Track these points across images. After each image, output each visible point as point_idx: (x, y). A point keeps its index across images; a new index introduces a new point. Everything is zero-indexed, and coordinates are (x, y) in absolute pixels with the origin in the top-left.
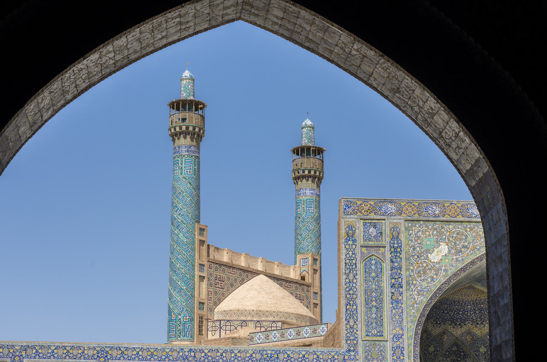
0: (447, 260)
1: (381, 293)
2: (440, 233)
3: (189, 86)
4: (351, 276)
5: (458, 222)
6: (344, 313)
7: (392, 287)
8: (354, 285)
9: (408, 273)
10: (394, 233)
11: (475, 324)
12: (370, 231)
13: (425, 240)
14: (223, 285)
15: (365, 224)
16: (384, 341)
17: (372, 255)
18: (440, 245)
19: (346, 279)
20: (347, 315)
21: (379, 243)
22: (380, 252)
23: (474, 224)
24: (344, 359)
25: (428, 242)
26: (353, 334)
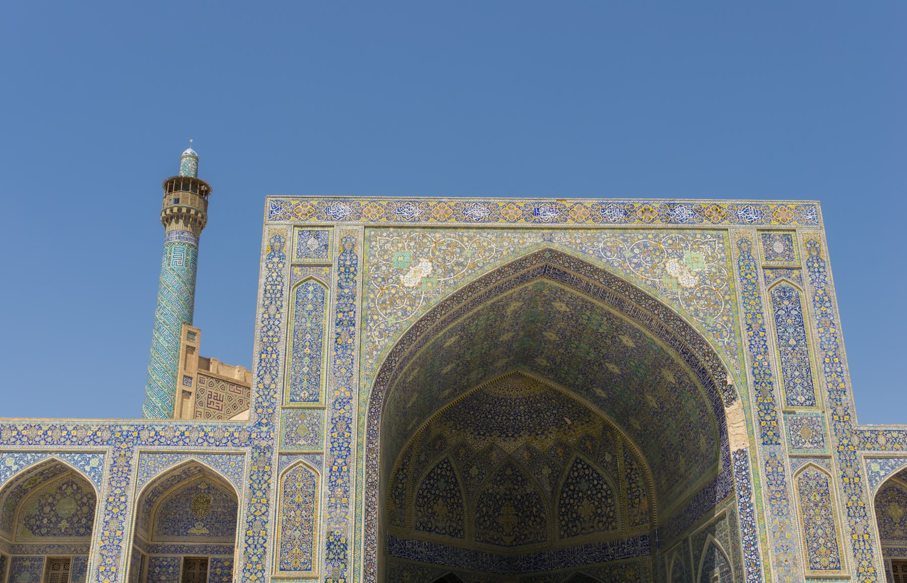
0: (429, 285)
1: (321, 335)
2: (420, 245)
6: (256, 366)
7: (337, 325)
8: (277, 323)
9: (365, 304)
10: (346, 246)
11: (534, 434)
13: (396, 254)
15: (301, 234)
16: (320, 408)
17: (309, 279)
19: (265, 313)
21: (322, 261)
24: (250, 438)
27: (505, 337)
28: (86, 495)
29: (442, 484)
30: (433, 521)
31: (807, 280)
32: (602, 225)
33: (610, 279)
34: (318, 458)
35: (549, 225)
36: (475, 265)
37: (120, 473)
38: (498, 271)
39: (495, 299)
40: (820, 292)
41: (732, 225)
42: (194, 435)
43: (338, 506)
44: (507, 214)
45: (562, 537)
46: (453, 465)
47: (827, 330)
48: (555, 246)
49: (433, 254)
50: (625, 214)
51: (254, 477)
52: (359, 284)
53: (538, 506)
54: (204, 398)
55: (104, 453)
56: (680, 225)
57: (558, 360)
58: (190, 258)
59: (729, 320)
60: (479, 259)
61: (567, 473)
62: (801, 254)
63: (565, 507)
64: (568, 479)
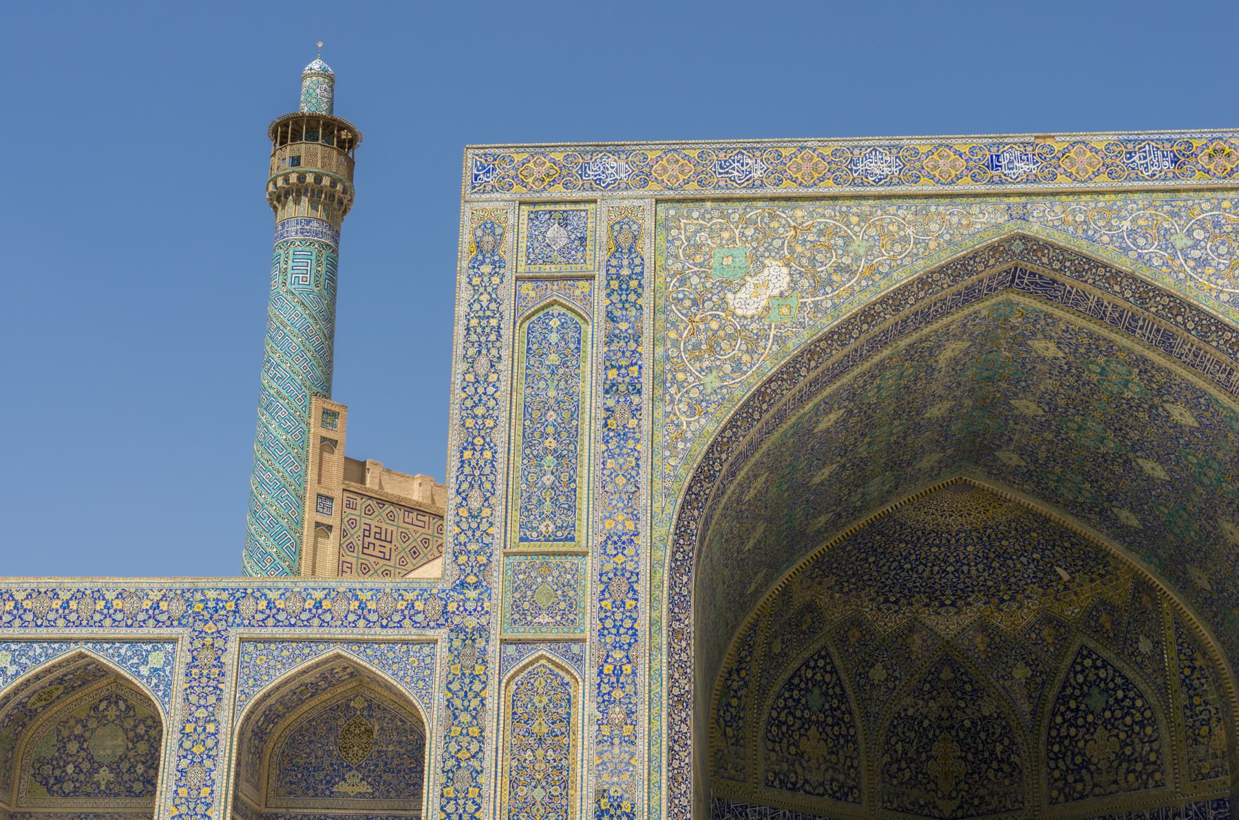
0: (785, 310)
1: (576, 412)
2: (765, 233)
3: (318, 91)
4: (482, 364)
5: (822, 198)
6: (454, 474)
7: (607, 392)
8: (491, 390)
9: (660, 350)
10: (621, 238)
12: (549, 234)
13: (718, 253)
14: (387, 551)
16: (576, 554)
18: (764, 266)
19: (467, 372)
20: (462, 478)
21: (575, 269)
22: (577, 292)
23: (871, 202)
24: (445, 612)
26: (478, 534)
27: (936, 411)
28: (143, 721)
29: (815, 699)
30: (799, 770)
32: (1127, 185)
33: (1146, 291)
34: (575, 649)
36: (873, 270)
37: (204, 680)
38: (922, 281)
39: (915, 336)
42: (341, 607)
43: (616, 741)
44: (935, 167)
45: (1053, 802)
46: (837, 662)
48: (1034, 229)
49: (792, 250)
50: (1175, 161)
51: (455, 686)
52: (647, 313)
53: (1006, 742)
54: (356, 536)
55: (173, 641)
57: (1042, 455)
58: (323, 269)
60: (882, 258)
61: (1062, 676)
63: (1061, 743)
64: (1064, 688)
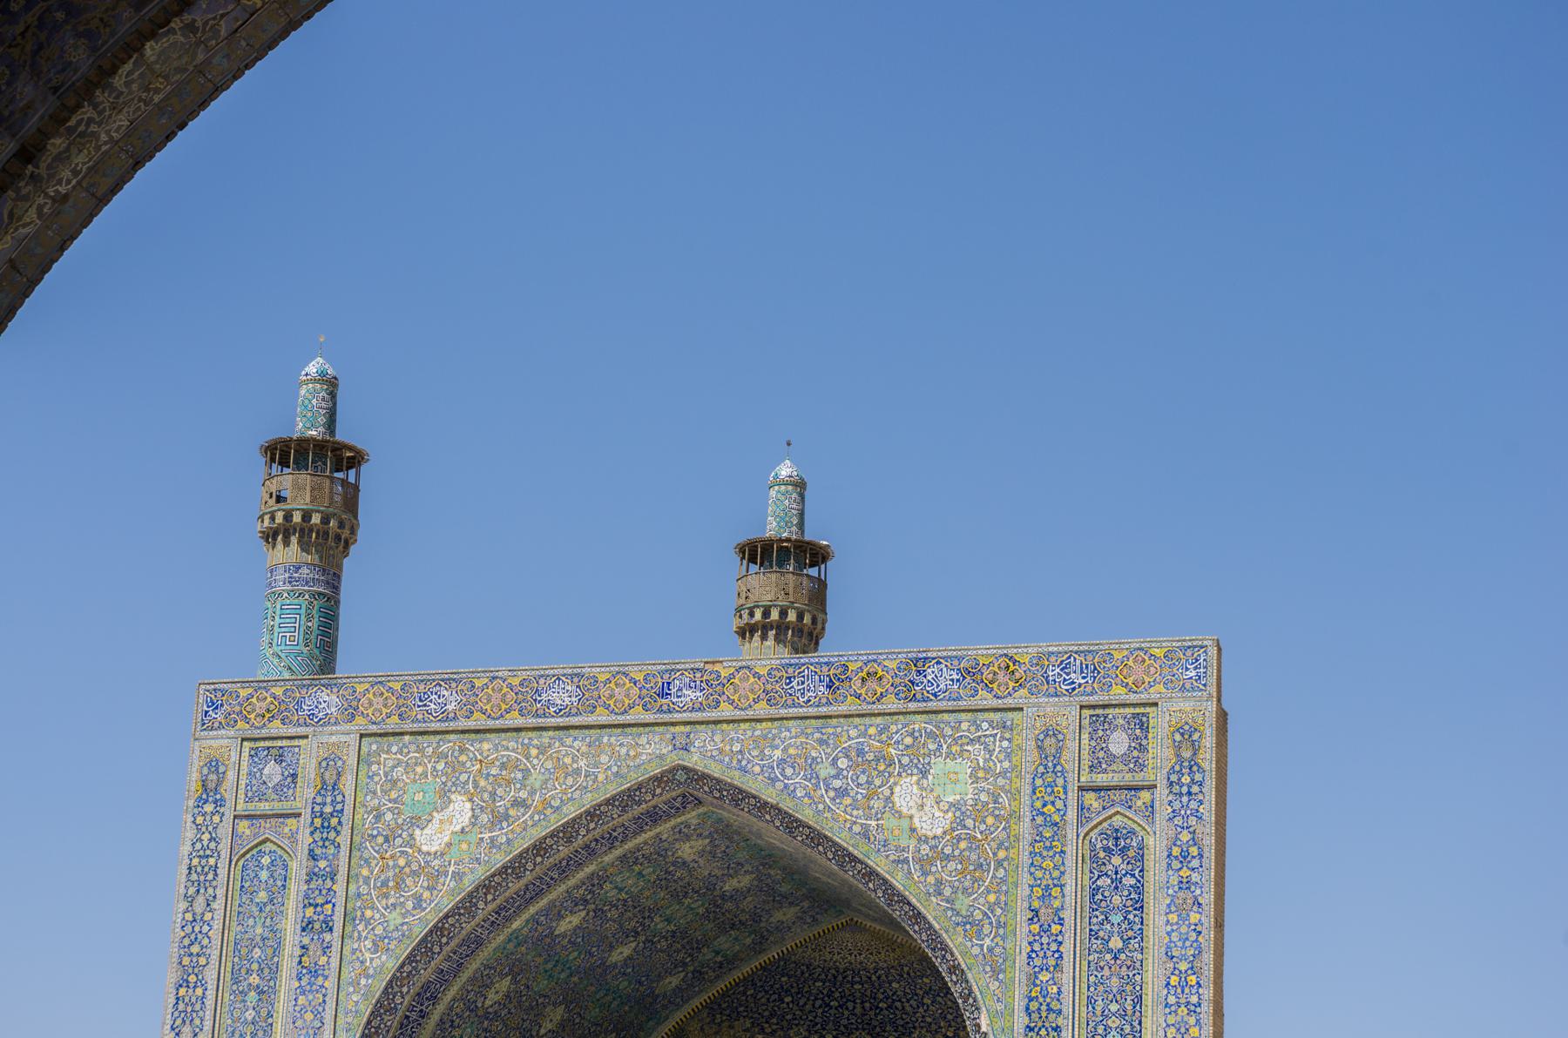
0: (464, 846)
1: (277, 950)
2: (455, 767)
3: (314, 402)
7: (303, 930)
8: (206, 928)
12: (266, 771)
13: (411, 789)
21: (285, 806)
22: (286, 830)
25: (417, 796)
31: (1164, 811)
32: (783, 712)
35: (686, 716)
36: (546, 804)
38: (588, 813)
40: (1185, 836)
41: (1033, 699)
44: (611, 697)
47: (1183, 919)
48: (694, 760)
56: (932, 705)
58: (314, 624)
59: (997, 903)
60: (555, 792)
62: (1160, 754)
